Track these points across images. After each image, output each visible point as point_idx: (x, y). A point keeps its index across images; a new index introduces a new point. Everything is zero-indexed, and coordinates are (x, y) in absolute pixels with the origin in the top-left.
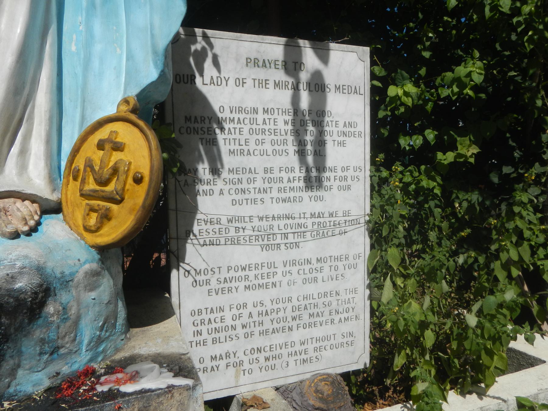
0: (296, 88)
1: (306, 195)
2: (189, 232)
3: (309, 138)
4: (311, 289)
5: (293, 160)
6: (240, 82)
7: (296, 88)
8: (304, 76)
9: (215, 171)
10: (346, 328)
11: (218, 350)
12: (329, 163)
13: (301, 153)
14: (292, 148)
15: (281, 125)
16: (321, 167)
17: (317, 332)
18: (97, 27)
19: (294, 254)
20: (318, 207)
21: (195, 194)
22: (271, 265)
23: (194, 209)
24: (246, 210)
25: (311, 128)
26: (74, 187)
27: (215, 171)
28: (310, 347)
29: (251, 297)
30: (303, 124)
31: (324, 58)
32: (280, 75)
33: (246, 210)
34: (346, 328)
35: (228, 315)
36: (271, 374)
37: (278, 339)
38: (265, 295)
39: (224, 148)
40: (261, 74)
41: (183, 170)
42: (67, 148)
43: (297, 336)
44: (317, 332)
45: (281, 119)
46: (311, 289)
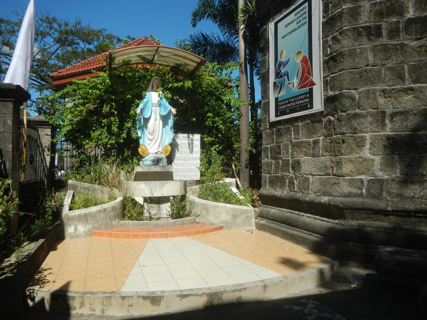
0: (189, 140)
1: (190, 154)
2: (174, 158)
3: (191, 147)
4: (191, 167)
5: (188, 150)
6: (181, 140)
7: (189, 140)
8: (190, 139)
9: (178, 151)
10: (196, 173)
11: (178, 174)
12: (194, 150)
13: (190, 149)
14: (188, 148)
15: (187, 145)
16: (193, 151)
17: (192, 173)
18: (166, 137)
19: (188, 162)
20: (192, 156)
21: (175, 154)
22: (185, 163)
23: (175, 155)
24: (182, 156)
25: (191, 145)
26: (164, 151)
27: (178, 151)
28: (191, 175)
29: (182, 167)
30: (190, 145)
31: (193, 136)
32: (187, 139)
33: (182, 156)
34: (196, 173)
35: (179, 169)
36: (185, 178)
37: (186, 174)
38: (184, 167)
39: (179, 148)
40: (184, 139)
41: (173, 150)
42: (163, 148)
43: (189, 173)
44: (192, 173)
45: (187, 144)
46: (191, 167)
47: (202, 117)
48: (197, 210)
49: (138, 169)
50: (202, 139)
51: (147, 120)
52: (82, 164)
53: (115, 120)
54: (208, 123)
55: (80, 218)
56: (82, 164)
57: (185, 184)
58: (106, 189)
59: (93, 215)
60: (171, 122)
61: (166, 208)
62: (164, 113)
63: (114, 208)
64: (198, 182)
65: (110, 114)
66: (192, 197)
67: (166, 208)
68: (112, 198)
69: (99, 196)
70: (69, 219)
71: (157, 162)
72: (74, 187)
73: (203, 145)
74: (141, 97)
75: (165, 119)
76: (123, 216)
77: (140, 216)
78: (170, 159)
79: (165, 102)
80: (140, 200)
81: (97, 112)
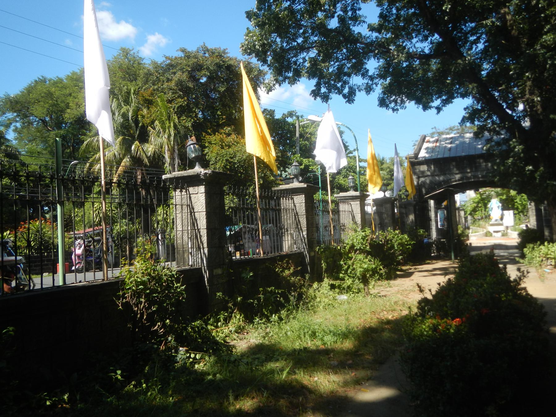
47: (513, 205)
48: (509, 234)
49: (491, 223)
50: (514, 212)
51: (492, 208)
52: (474, 221)
53: (483, 209)
54: (516, 207)
55: (475, 236)
56: (474, 221)
57: (507, 228)
58: (481, 229)
59: (477, 235)
60: (500, 208)
61: (499, 234)
62: (498, 206)
63: (483, 234)
64: (513, 226)
65: (481, 207)
66: (509, 231)
67: (499, 234)
68: (483, 231)
69: (479, 231)
70: (471, 236)
71: (496, 220)
72: (472, 228)
73: (514, 214)
74: (489, 201)
75: (498, 207)
76: (487, 236)
77: (491, 235)
78: (502, 219)
79: (498, 202)
80: (492, 232)
81: (477, 206)
